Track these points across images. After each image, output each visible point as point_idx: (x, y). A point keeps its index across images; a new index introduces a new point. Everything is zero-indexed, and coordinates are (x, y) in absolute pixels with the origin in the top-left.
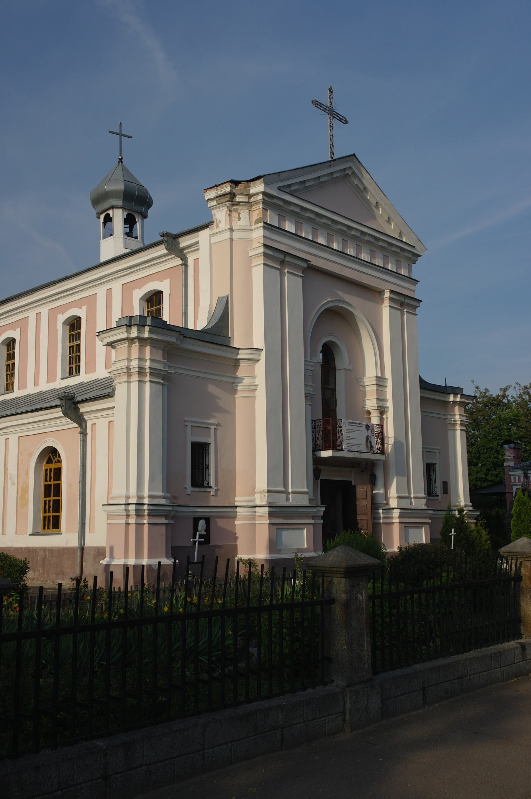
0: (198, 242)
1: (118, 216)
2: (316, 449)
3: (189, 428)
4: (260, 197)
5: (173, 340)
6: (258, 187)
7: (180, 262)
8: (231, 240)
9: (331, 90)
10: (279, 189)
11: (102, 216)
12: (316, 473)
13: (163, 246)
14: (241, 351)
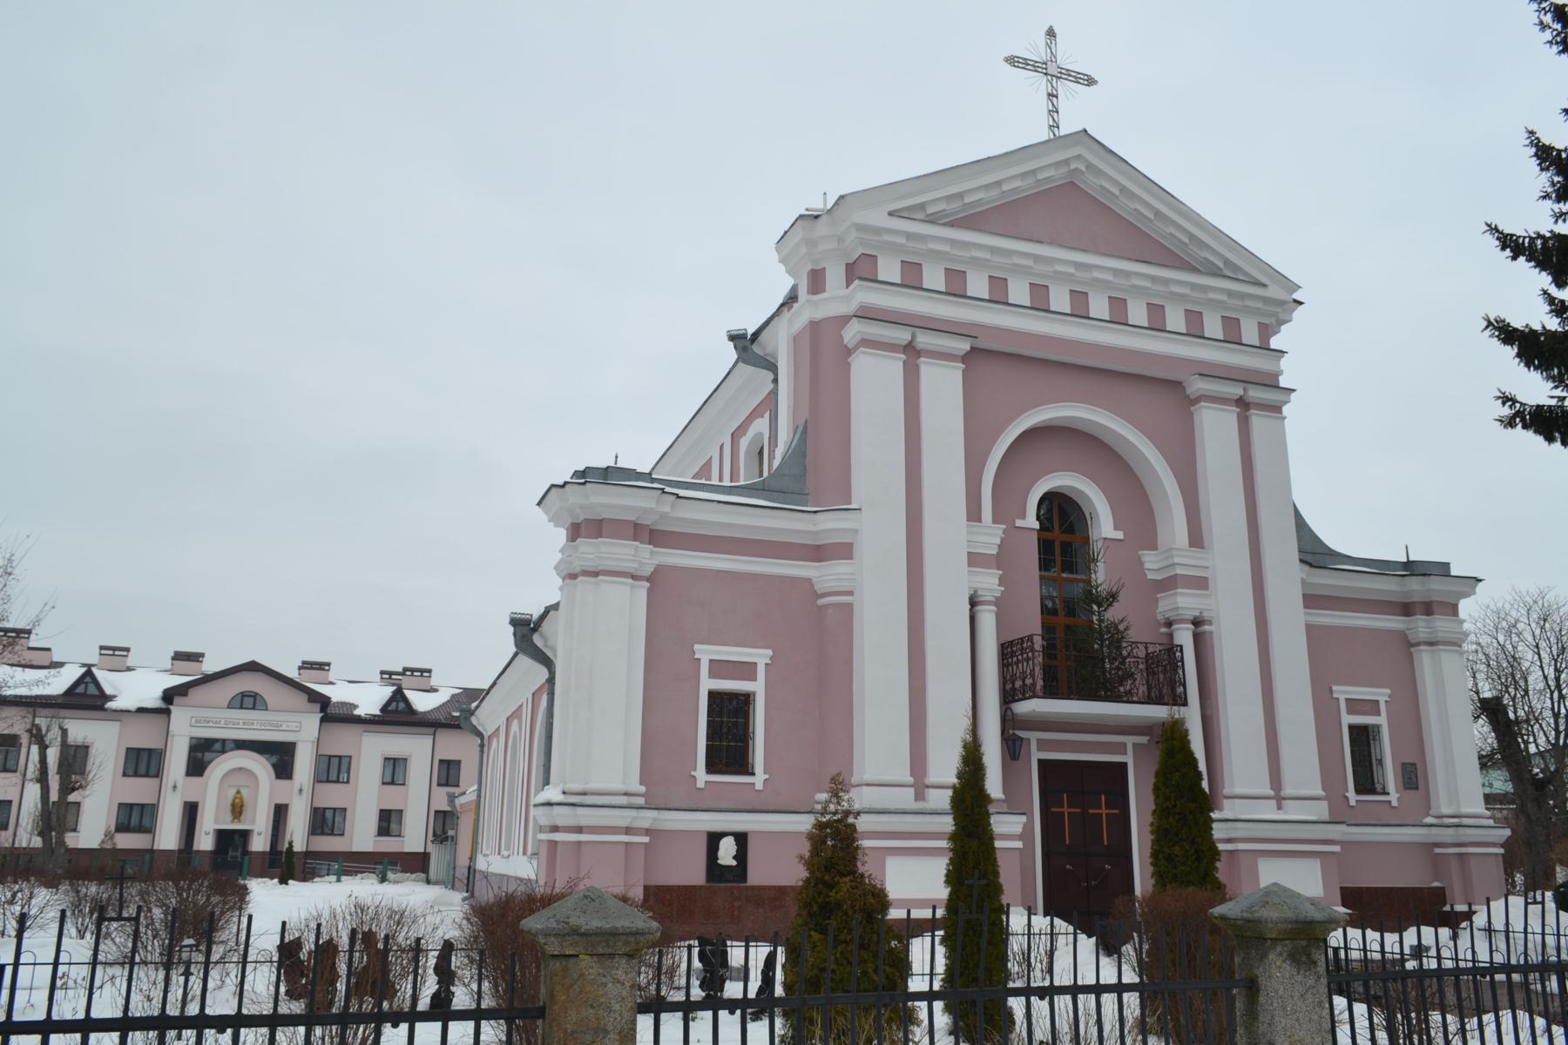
2: (1008, 696)
9: (1051, 33)
10: (891, 214)
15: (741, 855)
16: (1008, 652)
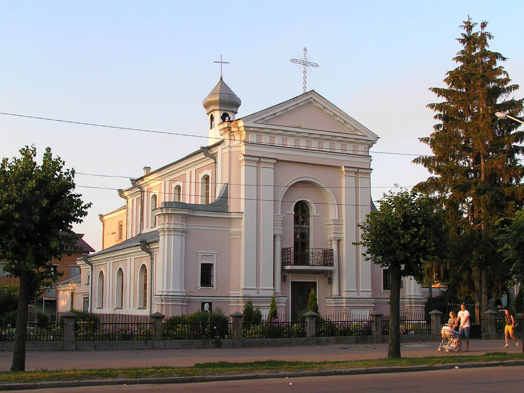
0: (217, 152)
1: (217, 115)
2: (283, 264)
3: (200, 256)
4: (243, 128)
5: (187, 213)
6: (241, 124)
7: (214, 161)
8: (230, 152)
9: (305, 49)
11: (210, 115)
12: (284, 278)
13: (202, 153)
14: (232, 214)
15: (210, 308)
16: (284, 251)
